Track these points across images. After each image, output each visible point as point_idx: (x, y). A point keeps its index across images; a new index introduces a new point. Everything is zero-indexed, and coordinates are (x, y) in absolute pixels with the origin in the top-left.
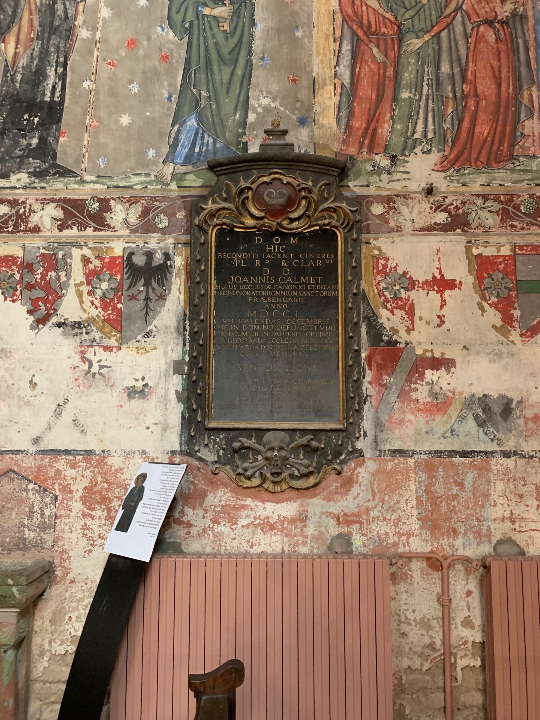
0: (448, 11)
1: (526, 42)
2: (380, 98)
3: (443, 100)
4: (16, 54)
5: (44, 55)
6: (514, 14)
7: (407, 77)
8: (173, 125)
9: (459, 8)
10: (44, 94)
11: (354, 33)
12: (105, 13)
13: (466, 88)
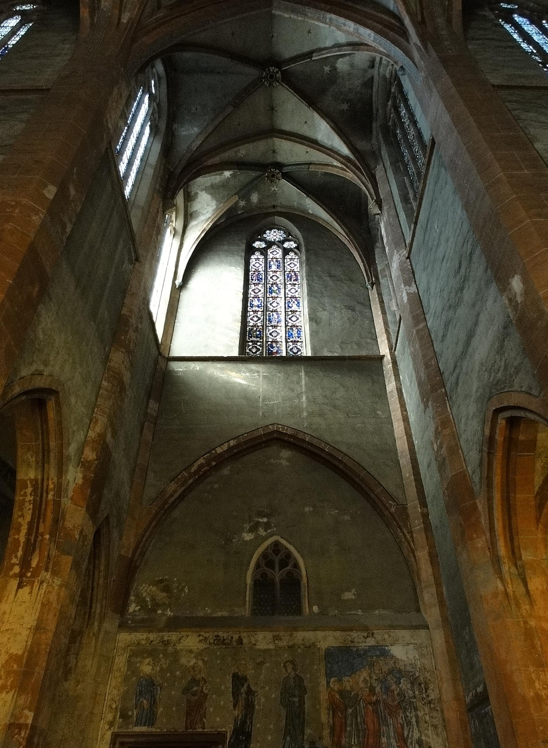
0: (358, 699)
1: (381, 710)
2: (341, 731)
3: (358, 730)
4: (238, 715)
5: (246, 715)
6: (377, 699)
7: (349, 722)
8: (283, 740)
9: (361, 699)
10: (246, 729)
11: (333, 706)
12: (263, 700)
13: (365, 726)
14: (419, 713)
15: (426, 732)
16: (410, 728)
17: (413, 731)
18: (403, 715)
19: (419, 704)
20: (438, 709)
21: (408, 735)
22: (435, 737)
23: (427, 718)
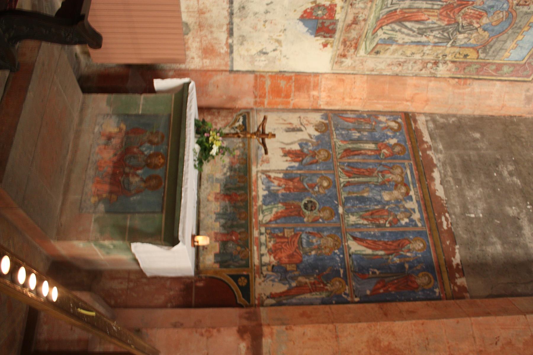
14: (430, 47)
15: (400, 52)
16: (414, 32)
17: (408, 35)
18: (435, 25)
19: (440, 50)
20: (424, 71)
21: (406, 27)
22: (389, 61)
23: (418, 57)
